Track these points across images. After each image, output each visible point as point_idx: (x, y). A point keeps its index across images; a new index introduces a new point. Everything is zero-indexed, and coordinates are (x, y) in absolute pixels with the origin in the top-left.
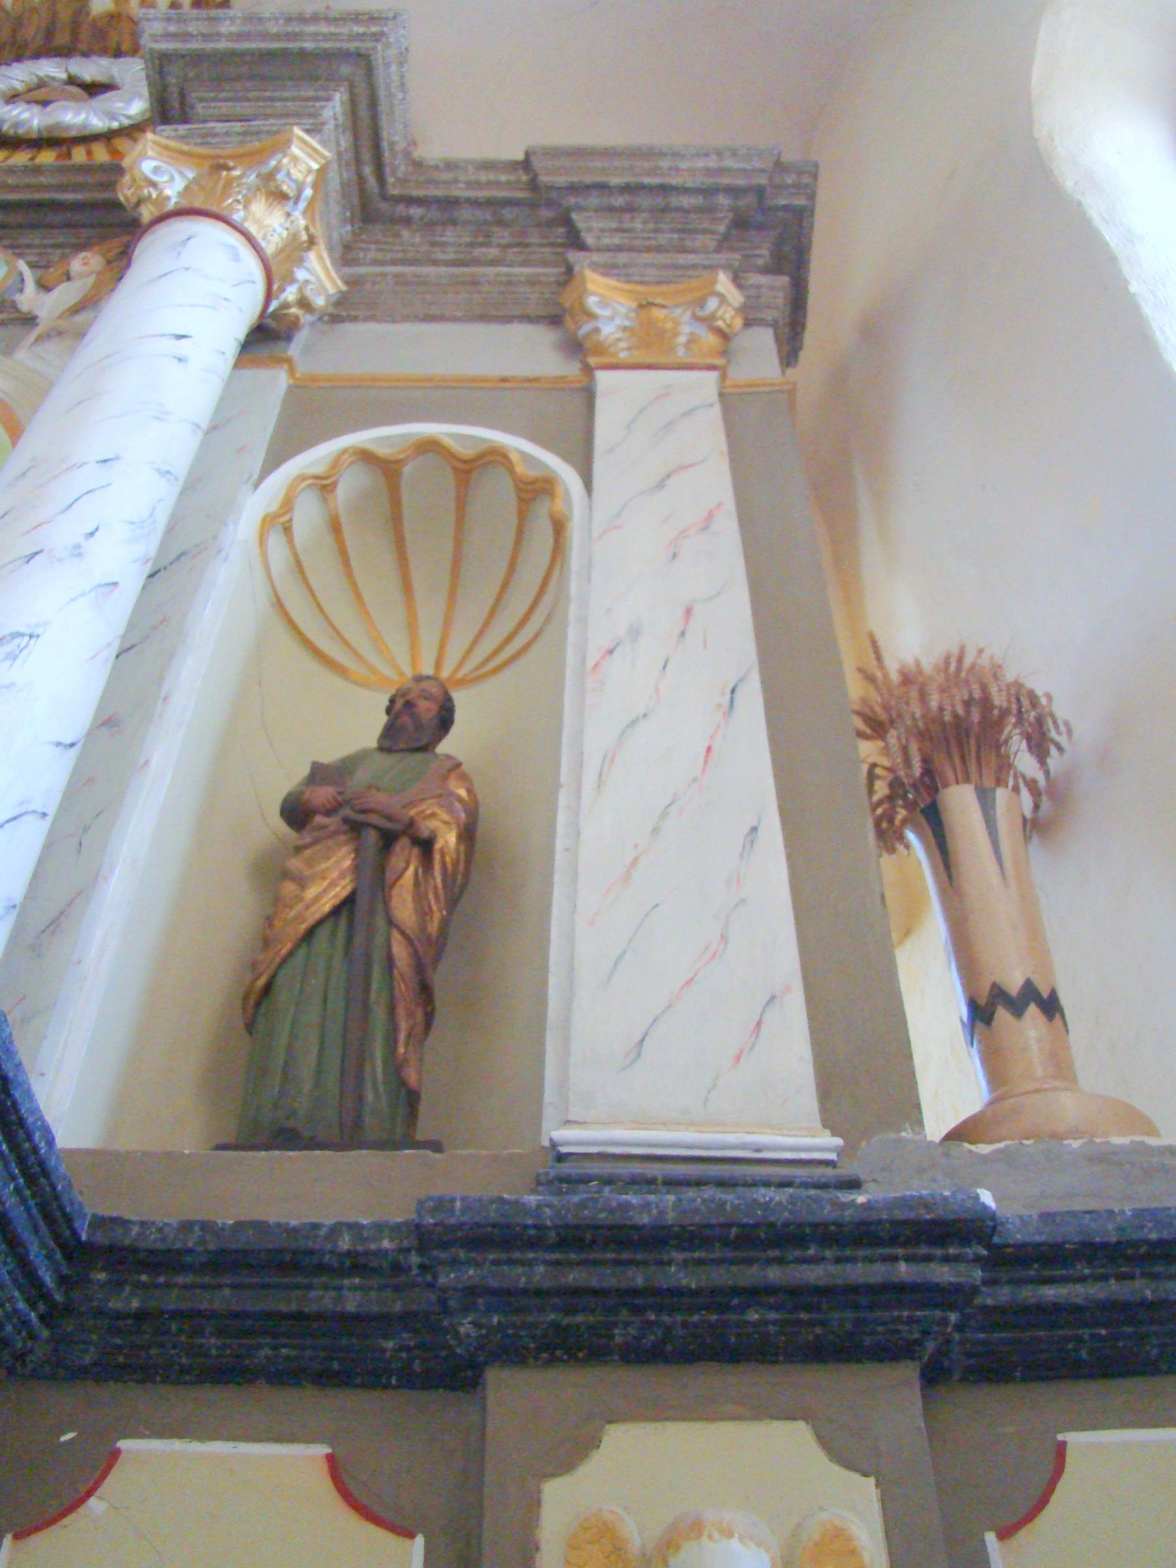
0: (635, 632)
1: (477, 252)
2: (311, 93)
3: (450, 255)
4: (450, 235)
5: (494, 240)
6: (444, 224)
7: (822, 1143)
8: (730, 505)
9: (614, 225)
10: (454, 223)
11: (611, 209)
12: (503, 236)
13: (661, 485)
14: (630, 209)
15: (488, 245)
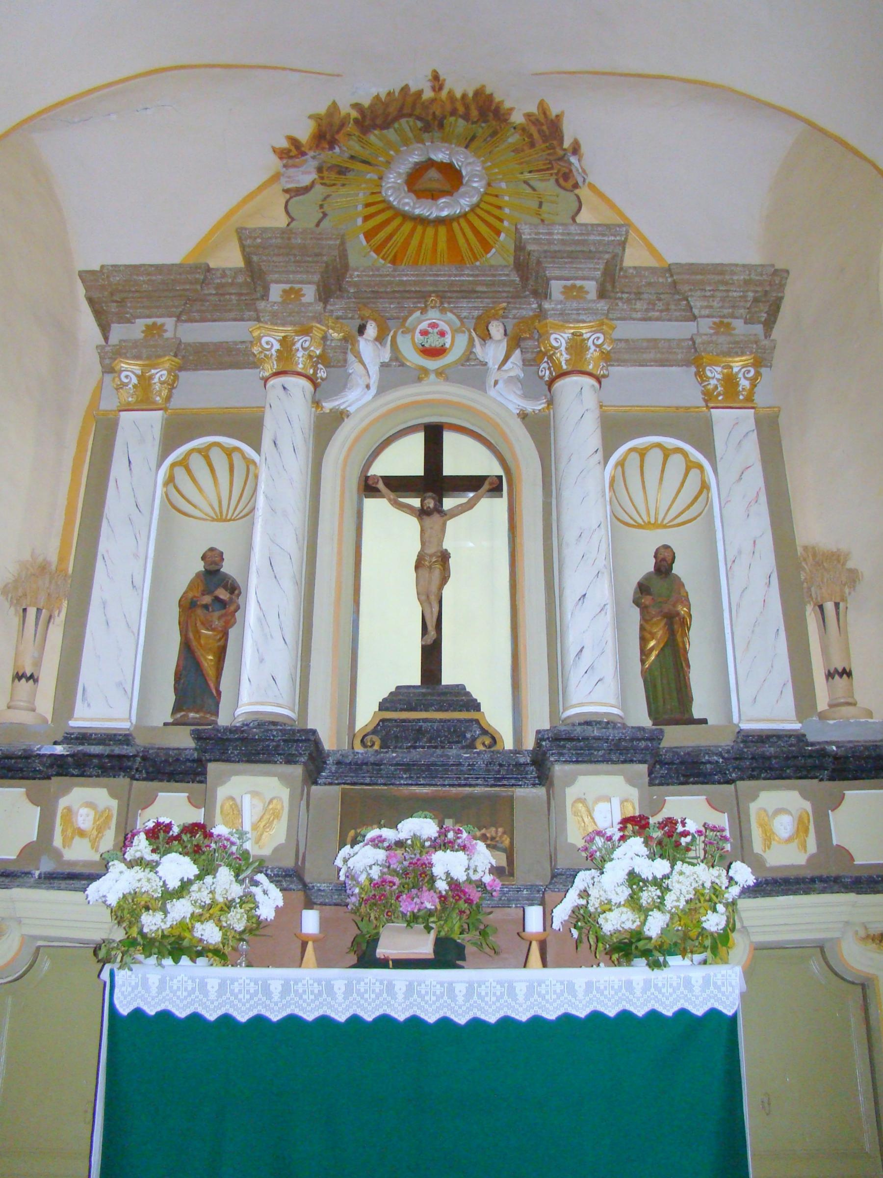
0: (740, 552)
1: (651, 314)
2: (592, 266)
3: (639, 315)
4: (638, 305)
5: (657, 308)
6: (636, 300)
7: (797, 726)
8: (763, 489)
9: (706, 304)
10: (640, 299)
11: (705, 296)
12: (660, 305)
13: (740, 479)
14: (713, 296)
15: (653, 310)
